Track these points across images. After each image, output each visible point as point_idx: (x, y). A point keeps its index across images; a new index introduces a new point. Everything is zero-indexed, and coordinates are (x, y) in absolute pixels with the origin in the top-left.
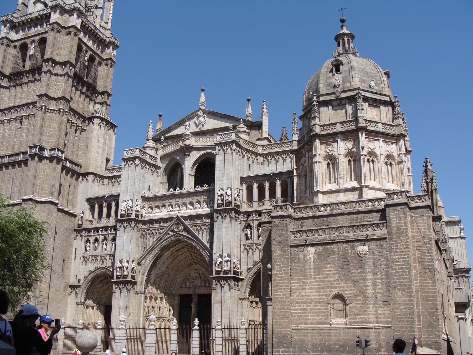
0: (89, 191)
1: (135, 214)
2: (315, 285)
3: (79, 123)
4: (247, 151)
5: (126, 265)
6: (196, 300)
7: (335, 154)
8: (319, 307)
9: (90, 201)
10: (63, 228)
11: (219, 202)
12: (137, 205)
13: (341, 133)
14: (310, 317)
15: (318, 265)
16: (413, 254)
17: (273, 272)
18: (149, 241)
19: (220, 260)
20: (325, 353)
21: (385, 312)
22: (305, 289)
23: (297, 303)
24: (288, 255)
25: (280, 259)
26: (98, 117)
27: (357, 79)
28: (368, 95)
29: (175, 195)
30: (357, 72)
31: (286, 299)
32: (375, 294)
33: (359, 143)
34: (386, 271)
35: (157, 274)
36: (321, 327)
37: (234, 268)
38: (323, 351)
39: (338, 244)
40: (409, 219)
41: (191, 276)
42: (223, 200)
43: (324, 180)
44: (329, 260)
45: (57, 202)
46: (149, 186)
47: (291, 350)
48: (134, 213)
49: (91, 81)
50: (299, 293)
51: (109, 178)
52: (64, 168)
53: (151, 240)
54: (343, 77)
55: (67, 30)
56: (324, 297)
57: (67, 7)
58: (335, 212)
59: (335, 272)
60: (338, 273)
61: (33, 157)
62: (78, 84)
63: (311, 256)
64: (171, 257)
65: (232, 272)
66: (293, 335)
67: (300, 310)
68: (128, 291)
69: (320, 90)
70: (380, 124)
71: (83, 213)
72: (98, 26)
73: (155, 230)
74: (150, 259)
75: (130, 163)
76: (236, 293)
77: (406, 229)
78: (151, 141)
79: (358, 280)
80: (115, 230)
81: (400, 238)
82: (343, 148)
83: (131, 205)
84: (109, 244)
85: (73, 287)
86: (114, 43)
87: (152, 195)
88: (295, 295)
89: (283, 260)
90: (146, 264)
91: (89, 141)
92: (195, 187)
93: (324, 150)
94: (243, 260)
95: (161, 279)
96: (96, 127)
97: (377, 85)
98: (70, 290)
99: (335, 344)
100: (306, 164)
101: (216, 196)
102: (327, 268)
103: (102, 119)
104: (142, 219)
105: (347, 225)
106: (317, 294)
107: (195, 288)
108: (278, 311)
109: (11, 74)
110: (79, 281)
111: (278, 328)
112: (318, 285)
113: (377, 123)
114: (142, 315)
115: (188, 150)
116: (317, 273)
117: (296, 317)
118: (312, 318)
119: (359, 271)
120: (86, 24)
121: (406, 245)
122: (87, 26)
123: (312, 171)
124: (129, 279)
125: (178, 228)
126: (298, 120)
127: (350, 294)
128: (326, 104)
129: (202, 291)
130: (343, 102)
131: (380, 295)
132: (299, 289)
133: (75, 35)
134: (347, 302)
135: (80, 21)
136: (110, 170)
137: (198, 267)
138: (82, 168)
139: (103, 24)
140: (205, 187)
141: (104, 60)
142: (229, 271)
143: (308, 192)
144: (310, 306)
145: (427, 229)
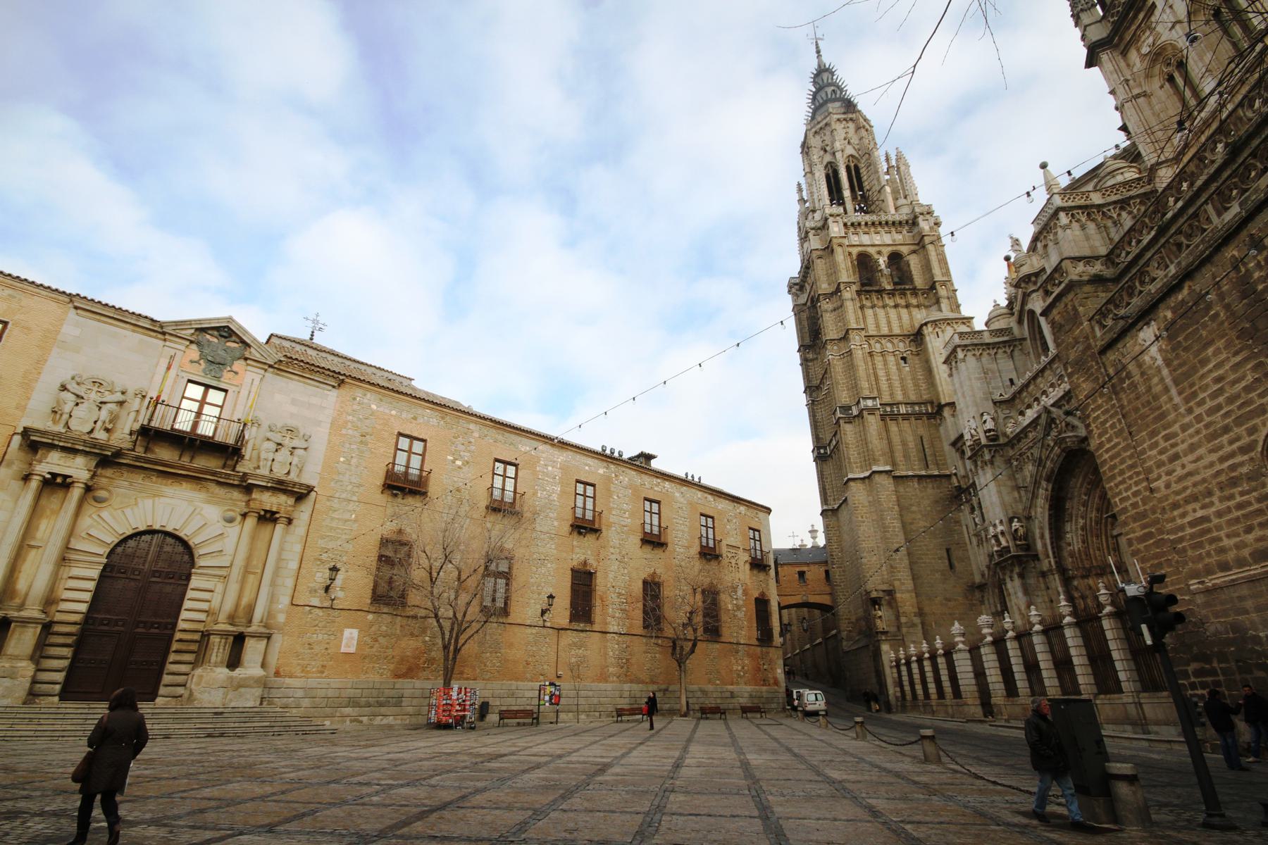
2: (1198, 432)
5: (1000, 528)
8: (1238, 499)
10: (926, 502)
14: (1226, 542)
15: (1180, 365)
17: (1094, 443)
22: (1176, 457)
23: (1175, 506)
26: (926, 324)
29: (1042, 371)
31: (1144, 504)
39: (1208, 266)
44: (1204, 333)
45: (888, 468)
46: (1011, 380)
50: (1169, 473)
53: (1030, 468)
56: (1239, 459)
57: (819, 224)
59: (1238, 358)
60: (1246, 360)
63: (1154, 350)
66: (1204, 612)
67: (1192, 524)
68: (1021, 576)
85: (981, 587)
88: (1160, 484)
90: (1039, 515)
98: (977, 594)
102: (1204, 362)
103: (935, 323)
106: (1214, 457)
108: (1141, 546)
112: (1207, 426)
116: (1188, 392)
117: (1190, 553)
124: (1013, 552)
135: (841, 225)
144: (1212, 504)
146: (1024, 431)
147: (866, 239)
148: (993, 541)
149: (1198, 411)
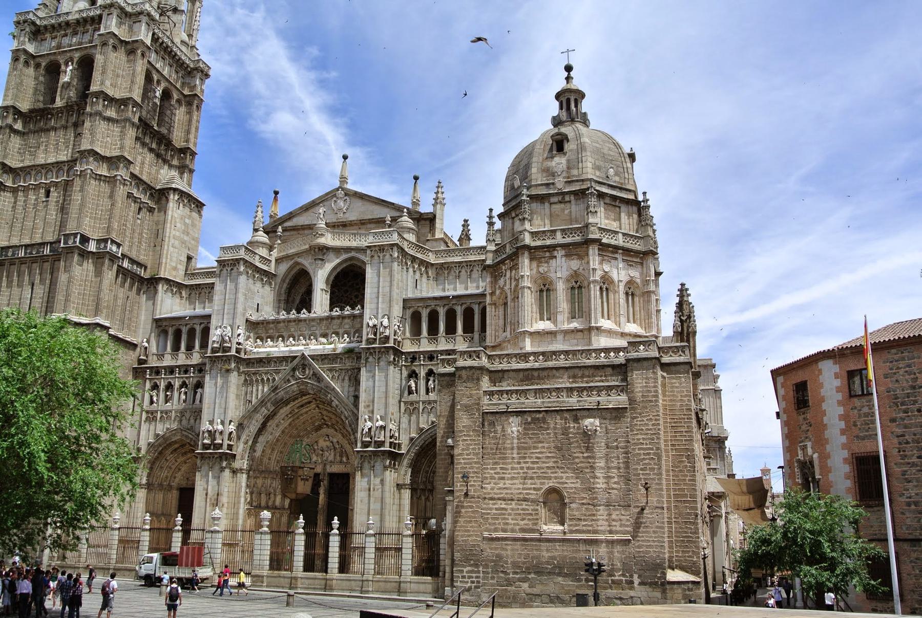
0: (159, 307)
2: (518, 473)
3: (145, 199)
4: (414, 259)
5: (220, 427)
6: (326, 482)
7: (552, 275)
9: (160, 323)
11: (370, 336)
12: (239, 335)
13: (563, 246)
14: (510, 521)
16: (665, 432)
17: (456, 451)
18: (257, 390)
19: (369, 424)
20: (533, 575)
21: (622, 517)
22: (503, 478)
23: (492, 499)
24: (479, 426)
26: (175, 190)
27: (589, 165)
28: (604, 190)
29: (300, 321)
30: (589, 154)
32: (608, 490)
33: (588, 263)
34: (625, 457)
35: (267, 442)
36: (527, 536)
37: (391, 437)
38: (530, 573)
40: (660, 380)
41: (320, 445)
42: (375, 334)
43: (534, 315)
45: (108, 325)
47: (481, 569)
48: (234, 346)
49: (164, 131)
50: (495, 484)
51: (191, 287)
52: (120, 270)
53: (261, 391)
54: (568, 161)
55: (129, 47)
58: (550, 364)
60: (553, 457)
61: (70, 250)
62: (145, 134)
63: (515, 429)
65: (387, 444)
67: (496, 509)
69: (533, 177)
70: (620, 235)
71: (148, 342)
72: (177, 41)
74: (259, 418)
75: (229, 269)
76: (390, 476)
77: (657, 396)
78: (261, 233)
79: (582, 468)
80: (200, 371)
81: (646, 408)
82: (564, 269)
83: (230, 334)
84: (190, 394)
86: (202, 71)
87: (261, 318)
91: (160, 227)
92: (331, 310)
93: (535, 270)
94: (404, 425)
95: (273, 450)
96: (172, 205)
97: (616, 174)
99: (548, 563)
100: (507, 288)
101: (365, 326)
102: (537, 448)
103: (182, 194)
104: (246, 357)
105: (568, 385)
106: (521, 486)
107: (325, 465)
109: (31, 111)
110: (139, 450)
111: (462, 536)
113: (616, 233)
114: (242, 505)
117: (490, 521)
118: (513, 522)
119: (585, 455)
120: (159, 38)
121: (656, 420)
122: (160, 41)
123: (516, 298)
124: (224, 450)
125: (304, 372)
126: (496, 220)
127: (572, 488)
128: (541, 199)
129: (336, 469)
130: (567, 198)
131: (616, 491)
132: (495, 479)
133: (143, 55)
134: (567, 501)
136: (193, 275)
137: (330, 431)
138: (148, 270)
139: (186, 38)
140: (348, 311)
141: (185, 96)
142: (384, 442)
143: (508, 329)
145: (686, 396)
147: (153, 57)
148: (206, 435)
149: (524, 465)
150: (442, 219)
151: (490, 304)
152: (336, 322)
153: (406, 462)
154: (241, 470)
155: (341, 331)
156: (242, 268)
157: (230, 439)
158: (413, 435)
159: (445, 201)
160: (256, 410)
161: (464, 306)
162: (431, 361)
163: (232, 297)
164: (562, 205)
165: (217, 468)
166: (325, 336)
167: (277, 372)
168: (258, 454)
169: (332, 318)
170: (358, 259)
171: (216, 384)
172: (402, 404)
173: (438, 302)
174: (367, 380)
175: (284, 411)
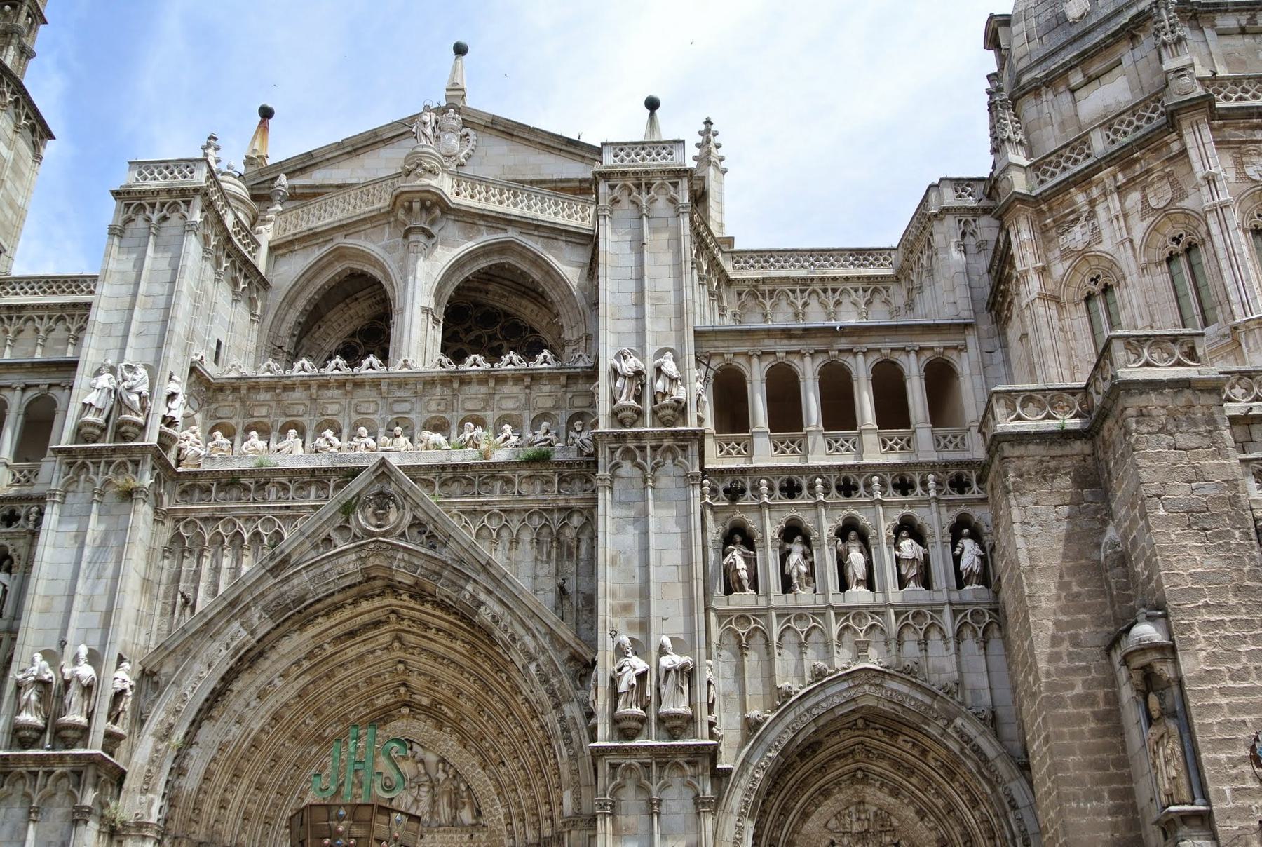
1: (161, 434)
5: (86, 671)
11: (623, 401)
18: (216, 570)
25: (1213, 594)
29: (359, 384)
46: (219, 344)
64: (306, 664)
73: (248, 519)
74: (217, 655)
75: (155, 217)
83: (144, 388)
89: (1233, 601)
115: (420, 213)
124: (95, 747)
137: (420, 728)
142: (691, 720)
146: (262, 479)
148: (31, 695)
150: (721, 203)
151: (1043, 297)
152: (474, 389)
153: (736, 799)
154: (140, 826)
155: (490, 416)
156: (197, 216)
157: (114, 717)
158: (754, 713)
159: (723, 165)
160: (208, 629)
161: (874, 358)
162: (791, 496)
163: (160, 290)
164: (1248, 40)
165: (58, 811)
166: (440, 427)
167: (291, 514)
168: (190, 783)
169: (464, 380)
170: (523, 252)
171: (80, 537)
172: (713, 616)
173: (795, 345)
174: (619, 530)
175: (295, 643)
